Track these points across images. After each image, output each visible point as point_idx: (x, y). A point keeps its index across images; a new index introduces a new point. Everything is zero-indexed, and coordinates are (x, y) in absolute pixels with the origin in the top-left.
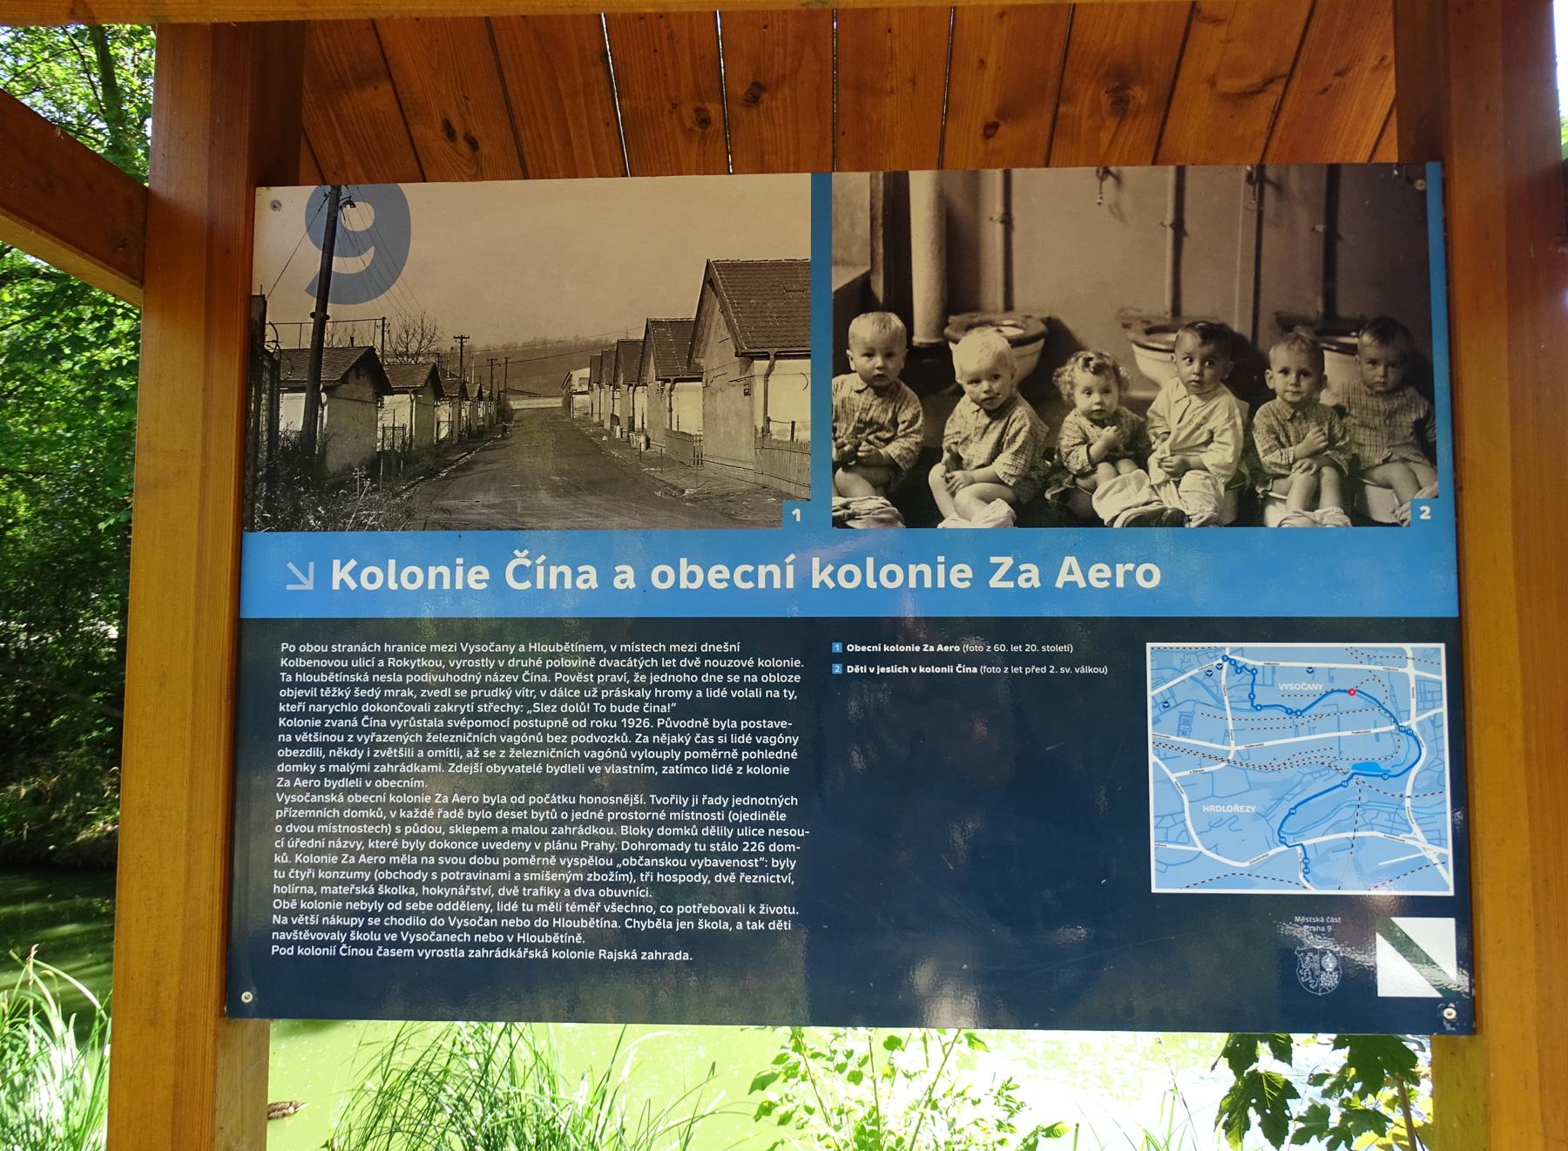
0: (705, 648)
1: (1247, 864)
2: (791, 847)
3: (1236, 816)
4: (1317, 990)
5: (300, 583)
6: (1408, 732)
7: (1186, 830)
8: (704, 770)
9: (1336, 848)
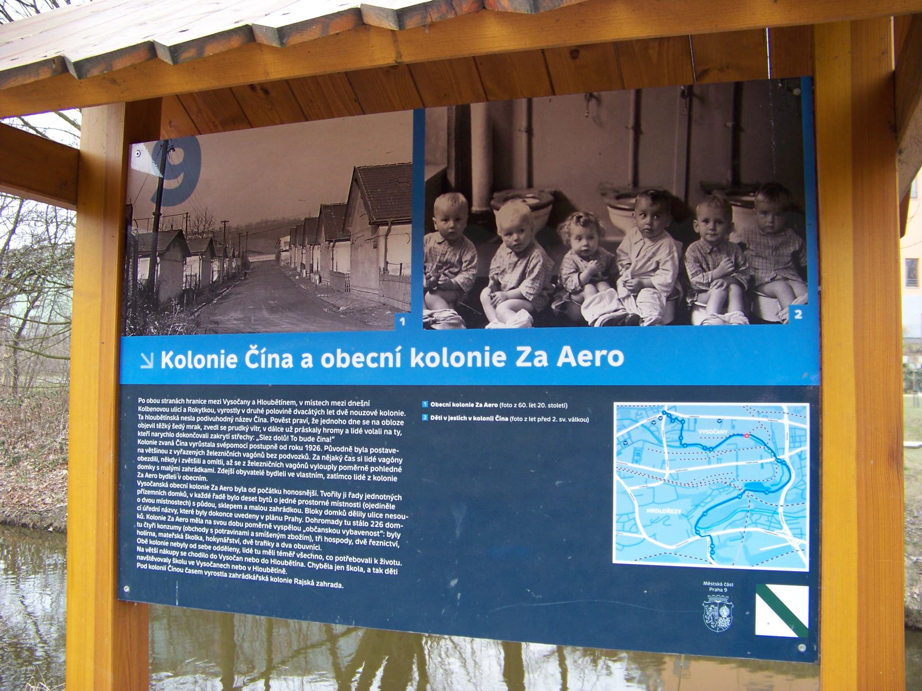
0: (351, 404)
1: (673, 547)
2: (398, 526)
4: (715, 629)
5: (147, 364)
6: (783, 463)
7: (636, 524)
8: (350, 477)
9: (733, 539)
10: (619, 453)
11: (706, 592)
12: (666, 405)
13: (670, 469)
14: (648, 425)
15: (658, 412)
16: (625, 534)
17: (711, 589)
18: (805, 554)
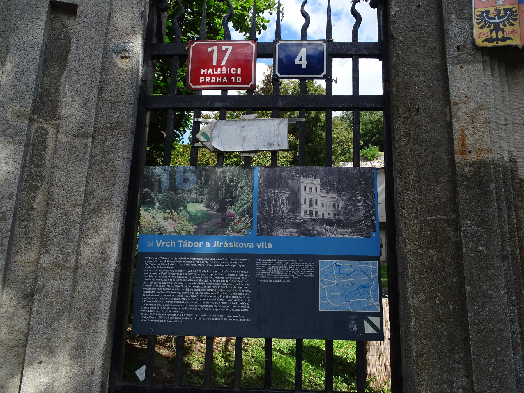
3: (337, 296)
6: (371, 279)
9: (357, 302)
12: (335, 261)
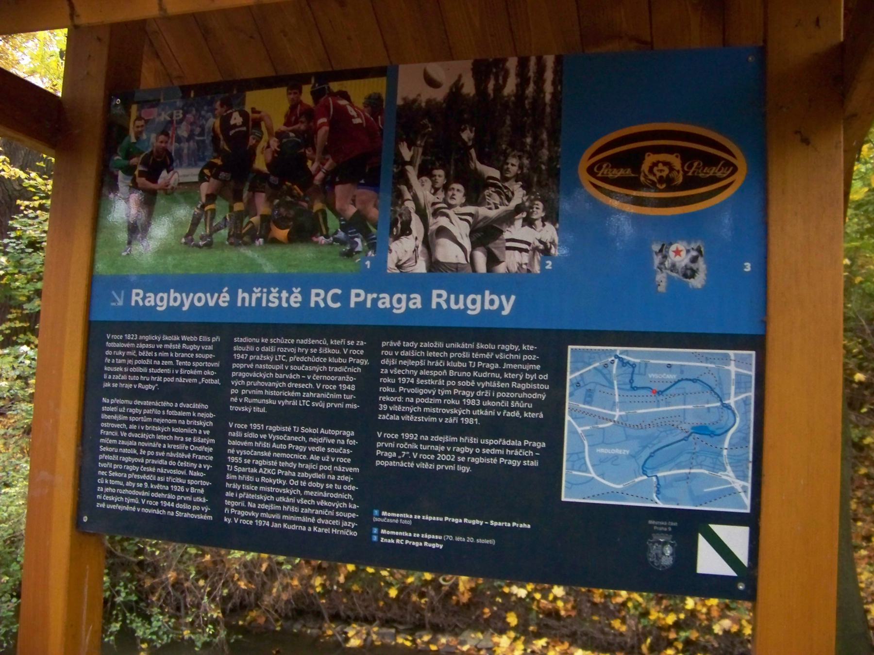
1: (620, 486)
3: (616, 456)
4: (658, 566)
5: (115, 301)
6: (728, 407)
7: (585, 463)
9: (678, 479)
10: (571, 395)
11: (651, 531)
12: (618, 349)
13: (620, 411)
14: (601, 368)
15: (611, 356)
16: (574, 473)
17: (655, 528)
18: (746, 496)
